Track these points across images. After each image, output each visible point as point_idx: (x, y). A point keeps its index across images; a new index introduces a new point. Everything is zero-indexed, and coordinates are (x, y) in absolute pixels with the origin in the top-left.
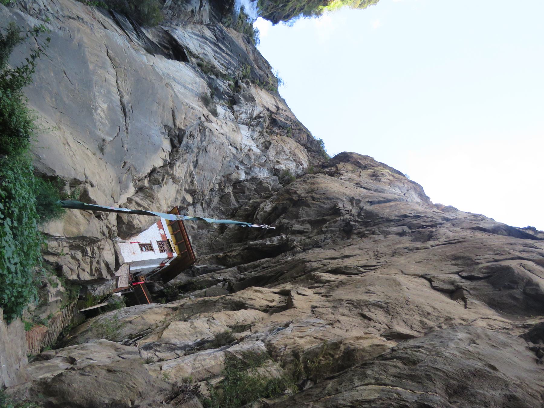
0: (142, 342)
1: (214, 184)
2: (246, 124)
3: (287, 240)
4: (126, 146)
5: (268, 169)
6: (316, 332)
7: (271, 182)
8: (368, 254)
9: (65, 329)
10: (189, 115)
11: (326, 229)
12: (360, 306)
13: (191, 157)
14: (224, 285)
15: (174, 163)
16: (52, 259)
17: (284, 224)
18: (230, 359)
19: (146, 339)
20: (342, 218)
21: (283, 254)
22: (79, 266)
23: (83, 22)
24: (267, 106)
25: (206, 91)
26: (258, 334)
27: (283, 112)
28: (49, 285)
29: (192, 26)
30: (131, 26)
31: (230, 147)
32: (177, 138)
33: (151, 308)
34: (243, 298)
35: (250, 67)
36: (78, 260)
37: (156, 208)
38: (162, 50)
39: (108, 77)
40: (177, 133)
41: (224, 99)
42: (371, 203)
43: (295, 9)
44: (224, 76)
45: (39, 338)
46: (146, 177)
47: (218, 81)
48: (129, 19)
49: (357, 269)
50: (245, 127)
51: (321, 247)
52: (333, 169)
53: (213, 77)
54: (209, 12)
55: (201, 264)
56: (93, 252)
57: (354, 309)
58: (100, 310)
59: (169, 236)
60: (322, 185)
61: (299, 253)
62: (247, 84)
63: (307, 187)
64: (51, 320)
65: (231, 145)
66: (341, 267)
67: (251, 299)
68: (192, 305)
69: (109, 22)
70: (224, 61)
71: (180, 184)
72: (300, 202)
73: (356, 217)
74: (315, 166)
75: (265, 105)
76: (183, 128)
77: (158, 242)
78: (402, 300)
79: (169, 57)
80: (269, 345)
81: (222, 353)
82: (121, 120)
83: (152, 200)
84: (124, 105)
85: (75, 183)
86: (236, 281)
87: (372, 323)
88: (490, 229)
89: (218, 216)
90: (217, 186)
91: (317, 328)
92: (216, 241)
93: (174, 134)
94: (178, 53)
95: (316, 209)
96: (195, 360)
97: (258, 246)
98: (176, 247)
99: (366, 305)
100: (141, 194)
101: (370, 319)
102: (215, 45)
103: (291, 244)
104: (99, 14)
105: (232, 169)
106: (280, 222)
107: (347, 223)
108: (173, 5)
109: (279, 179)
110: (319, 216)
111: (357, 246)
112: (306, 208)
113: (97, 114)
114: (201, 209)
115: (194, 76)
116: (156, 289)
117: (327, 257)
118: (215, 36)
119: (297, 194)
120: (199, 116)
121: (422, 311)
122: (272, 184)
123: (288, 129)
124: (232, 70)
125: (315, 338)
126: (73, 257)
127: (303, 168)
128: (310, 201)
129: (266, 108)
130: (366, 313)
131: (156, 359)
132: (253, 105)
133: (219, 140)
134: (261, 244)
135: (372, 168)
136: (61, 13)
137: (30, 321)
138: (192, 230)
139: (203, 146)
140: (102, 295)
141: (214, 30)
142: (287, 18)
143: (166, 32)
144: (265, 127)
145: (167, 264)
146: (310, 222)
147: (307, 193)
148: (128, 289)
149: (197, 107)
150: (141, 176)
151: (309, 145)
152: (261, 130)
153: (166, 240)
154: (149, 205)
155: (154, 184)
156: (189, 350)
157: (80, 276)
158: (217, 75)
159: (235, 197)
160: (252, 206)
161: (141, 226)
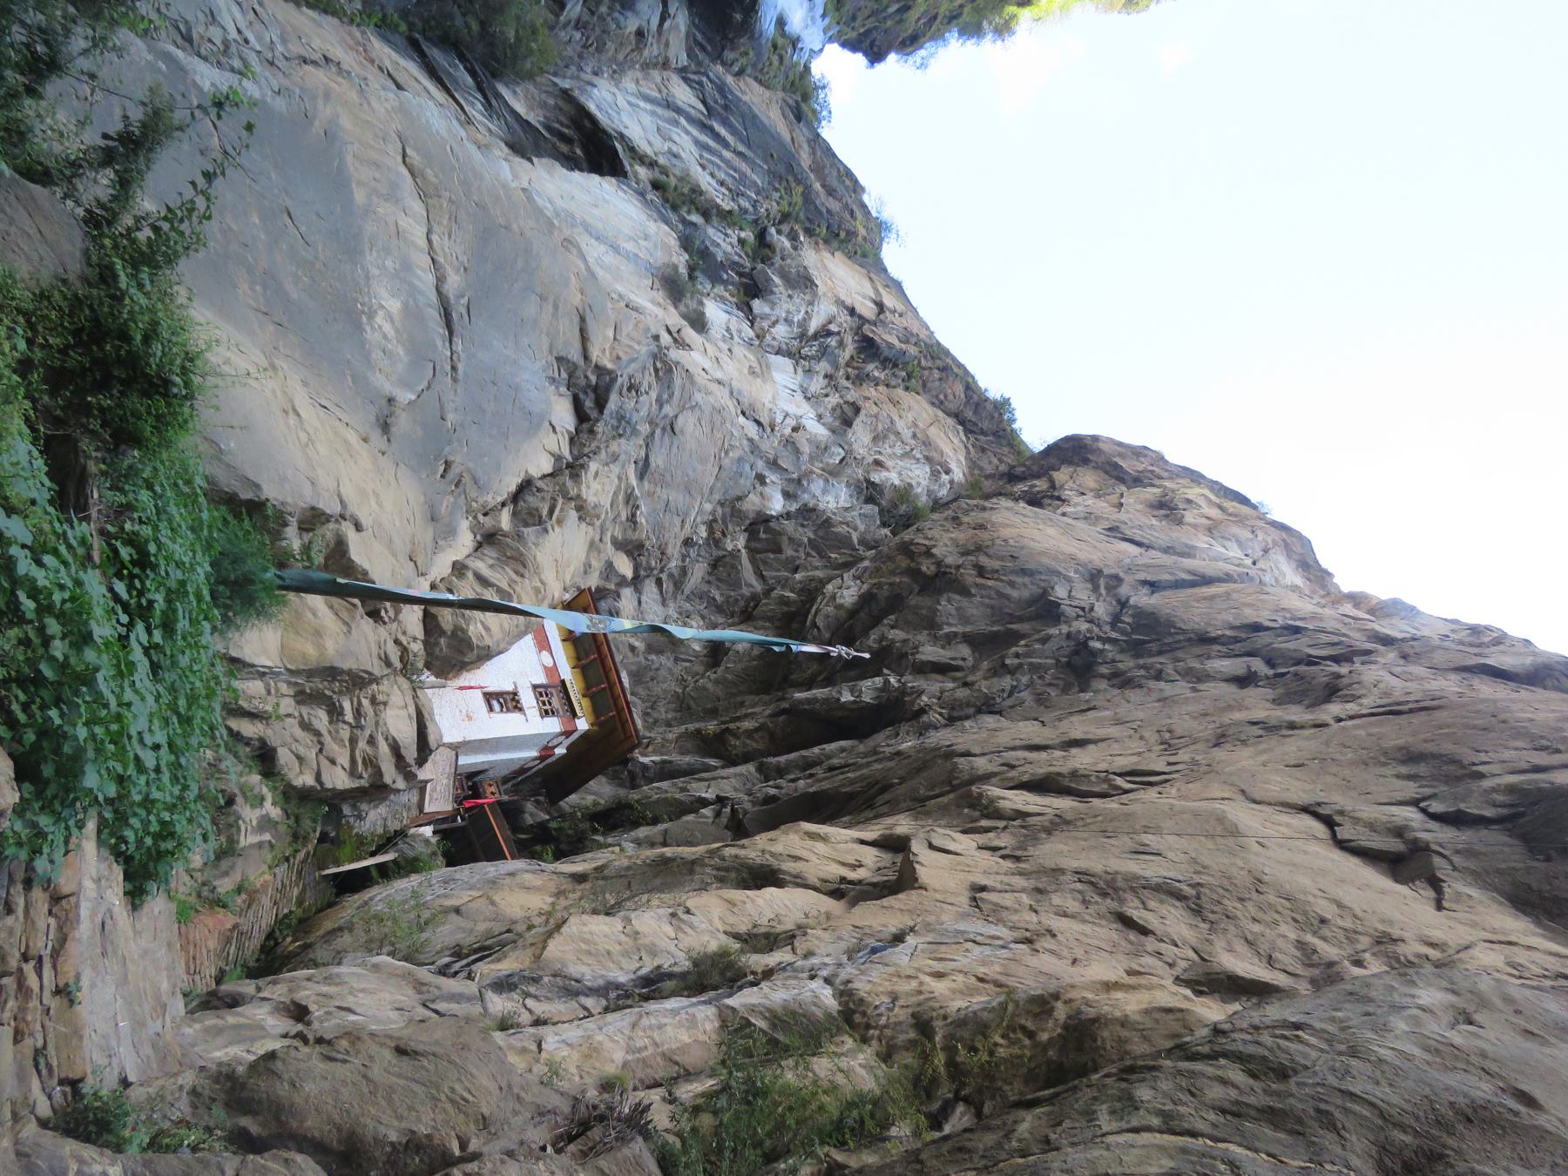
0: (487, 970)
1: (695, 526)
2: (789, 354)
3: (903, 691)
4: (450, 416)
5: (848, 485)
6: (984, 963)
7: (858, 522)
8: (1141, 738)
9: (282, 922)
10: (627, 328)
11: (1016, 661)
12: (1116, 890)
13: (630, 448)
14: (718, 814)
15: (582, 466)
16: (249, 729)
17: (893, 642)
18: (735, 1028)
19: (499, 960)
20: (1065, 629)
21: (888, 731)
22: (321, 750)
23: (340, 71)
24: (849, 302)
25: (675, 259)
26: (814, 961)
27: (896, 319)
28: (239, 800)
29: (639, 74)
30: (470, 81)
31: (741, 419)
32: (592, 395)
33: (512, 874)
34: (773, 855)
35: (800, 189)
36: (318, 734)
37: (532, 592)
38: (554, 145)
39: (404, 222)
40: (593, 379)
41: (725, 283)
42: (1154, 586)
43: (935, 17)
44: (726, 217)
45: (212, 944)
46: (503, 505)
47: (711, 231)
48: (462, 58)
49: (1106, 780)
50: (787, 363)
51: (1000, 713)
52: (1041, 485)
53: (695, 218)
54: (688, 34)
55: (655, 752)
56: (358, 713)
57: (1097, 898)
58: (374, 873)
59: (567, 673)
60: (1006, 533)
61: (936, 728)
62: (793, 237)
63: (961, 536)
64: (244, 896)
65: (743, 413)
66: (1059, 774)
67: (796, 858)
68: (628, 868)
69: (409, 69)
70: (727, 174)
71: (598, 523)
72: (941, 581)
73: (1107, 628)
74: (987, 477)
75: (843, 297)
76: (610, 366)
77: (535, 687)
78: (1242, 878)
79: (571, 163)
80: (845, 994)
81: (711, 1011)
82: (439, 343)
83: (522, 570)
84: (447, 299)
85: (313, 519)
86: (754, 804)
87: (1150, 944)
88: (1519, 670)
89: (703, 617)
90: (703, 532)
91: (987, 951)
92: (696, 688)
93: (583, 382)
94: (597, 151)
95: (987, 601)
96: (634, 1026)
97: (818, 706)
98: (586, 702)
99: (1132, 889)
100: (490, 552)
101: (1144, 931)
103: (912, 703)
105: (746, 483)
106: (883, 638)
107: (1080, 646)
108: (586, 17)
109: (881, 512)
110: (994, 623)
111: (1107, 713)
112: (957, 597)
113: (372, 328)
114: (658, 597)
115: (644, 217)
116: (529, 820)
117: (1018, 743)
118: (704, 102)
119: (933, 555)
120: (654, 331)
121: (1305, 913)
122: (862, 527)
123: (910, 368)
124: (748, 198)
125: (981, 980)
126: (306, 726)
127: (951, 482)
128: (969, 577)
129: (846, 308)
130: (1136, 913)
131: (525, 1018)
132: (807, 297)
133: (711, 399)
134: (826, 700)
135: (1156, 482)
136: (280, 48)
137: (193, 899)
138: (630, 654)
139: (666, 416)
140: (380, 831)
141: (700, 83)
142: (909, 43)
143: (566, 94)
144: (842, 361)
145: (560, 751)
146: (969, 639)
147: (963, 554)
148: (451, 817)
149: (649, 305)
150: (493, 499)
151: (969, 414)
152: (830, 370)
153: (557, 682)
154: (512, 583)
155: (527, 525)
156: (619, 997)
157: (325, 778)
158: (706, 215)
159: (753, 561)
160: (802, 590)
161: (488, 641)
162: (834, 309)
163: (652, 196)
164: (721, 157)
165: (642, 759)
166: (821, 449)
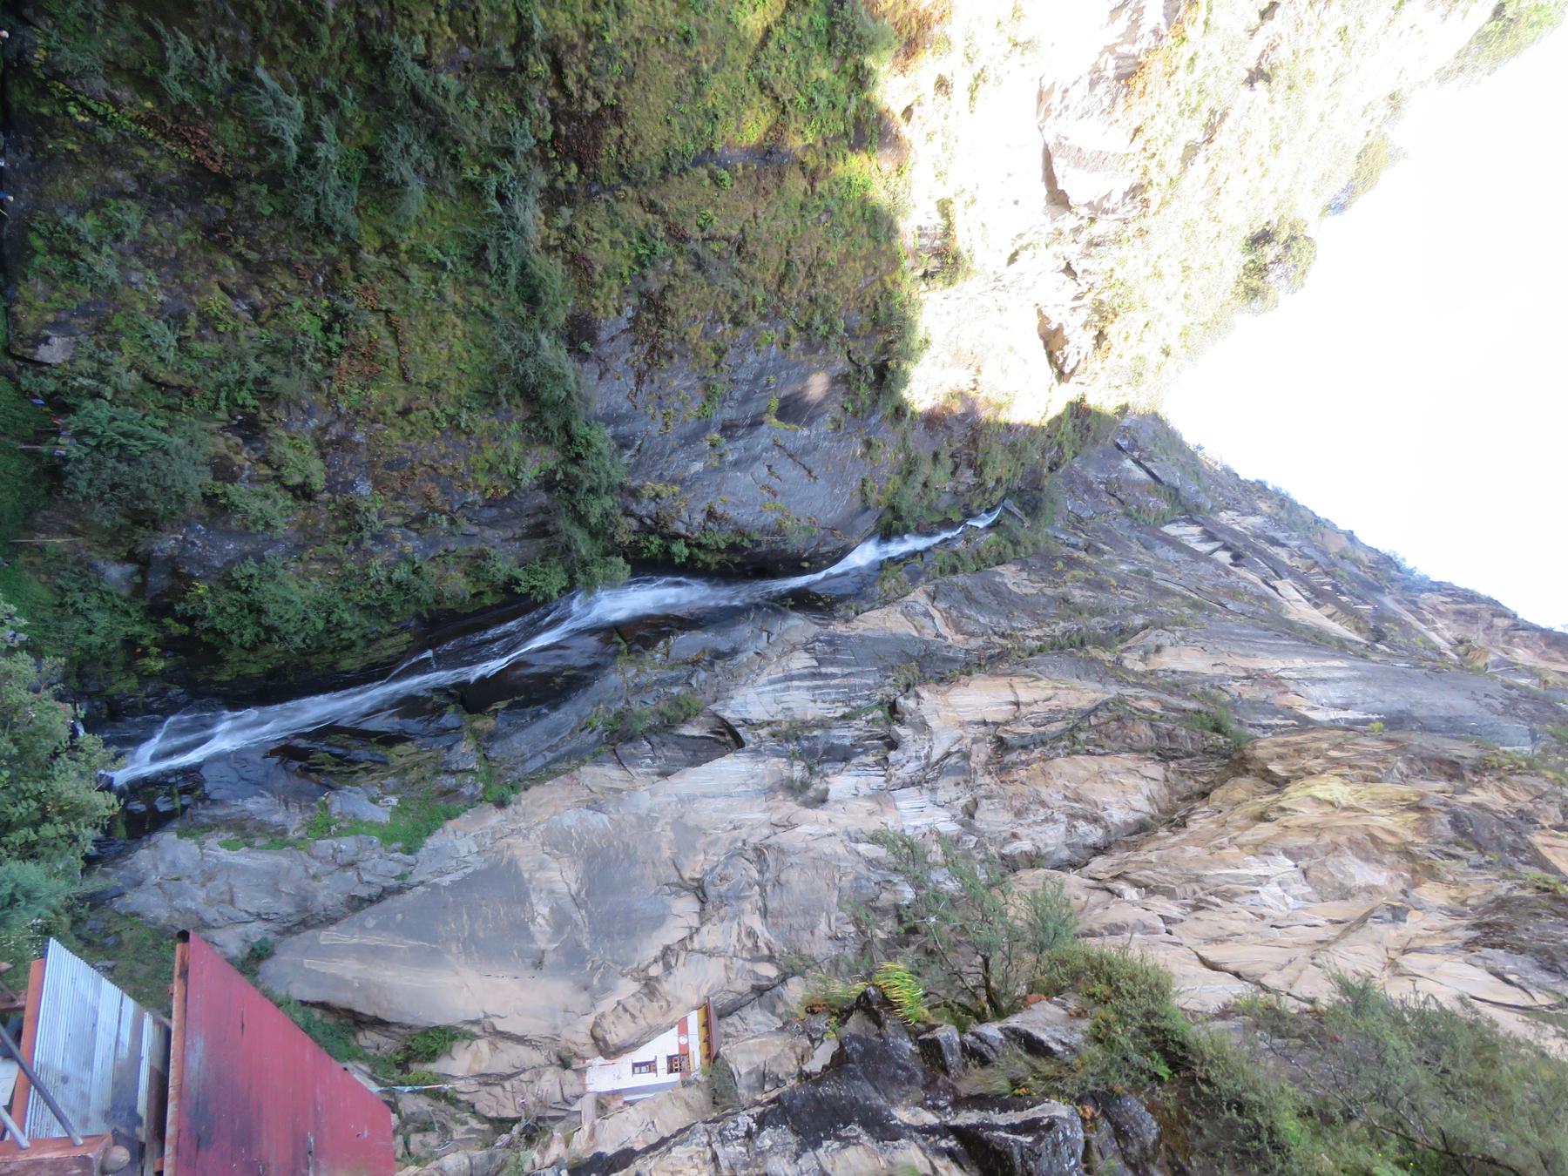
2: (913, 784)
16: (463, 1097)
24: (979, 717)
25: (786, 773)
31: (862, 848)
38: (716, 741)
39: (550, 874)
41: (866, 752)
47: (835, 732)
76: (698, 876)
77: (670, 1059)
90: (851, 929)
94: (728, 738)
102: (813, 676)
143: (715, 715)
162: (961, 732)
163: (771, 744)
164: (829, 686)
166: (950, 843)
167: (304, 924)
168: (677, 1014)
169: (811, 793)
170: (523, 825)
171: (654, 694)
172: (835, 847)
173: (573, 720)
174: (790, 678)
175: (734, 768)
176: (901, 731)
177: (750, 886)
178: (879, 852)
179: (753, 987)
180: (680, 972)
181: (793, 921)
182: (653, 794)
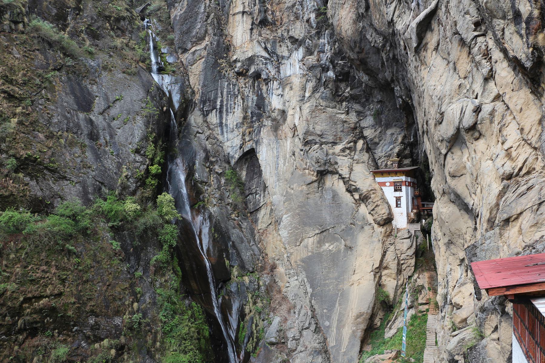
30: (250, 196)
31: (307, 95)
39: (310, 244)
40: (319, 175)
47: (250, 104)
50: (282, 68)
55: (411, 137)
70: (231, 100)
76: (315, 174)
77: (396, 190)
90: (344, 103)
92: (391, 107)
94: (250, 157)
102: (221, 112)
104: (261, 225)
115: (264, 146)
118: (212, 110)
129: (251, 33)
141: (207, 111)
143: (237, 163)
164: (227, 104)
165: (412, 140)
166: (309, 52)
167: (326, 352)
168: (377, 186)
169: (279, 117)
170: (285, 256)
171: (224, 191)
172: (307, 107)
173: (236, 231)
174: (221, 123)
175: (265, 154)
176: (252, 70)
177: (322, 149)
178: (310, 86)
179: (367, 152)
180: (359, 185)
181: (339, 130)
182: (275, 194)
